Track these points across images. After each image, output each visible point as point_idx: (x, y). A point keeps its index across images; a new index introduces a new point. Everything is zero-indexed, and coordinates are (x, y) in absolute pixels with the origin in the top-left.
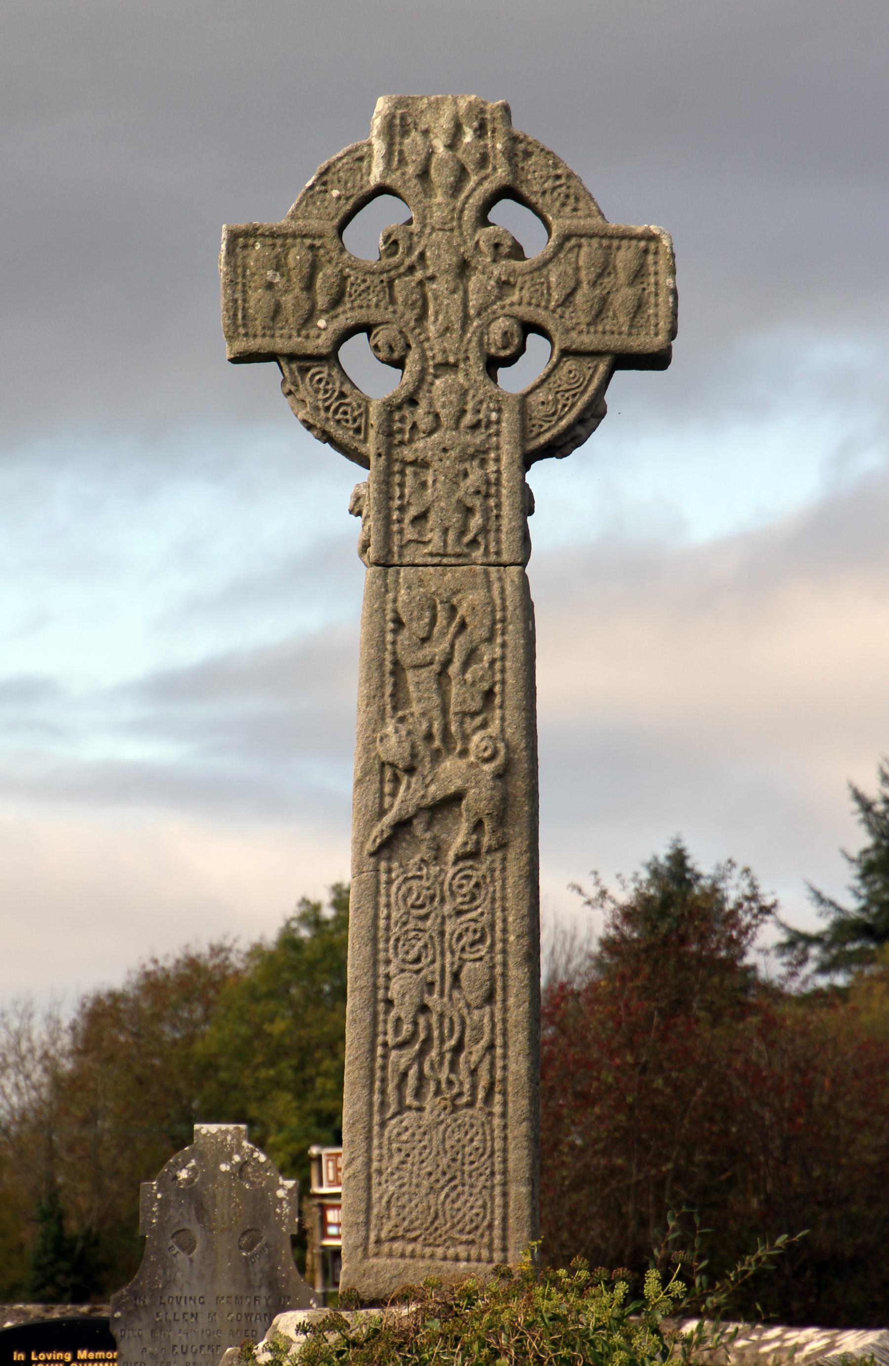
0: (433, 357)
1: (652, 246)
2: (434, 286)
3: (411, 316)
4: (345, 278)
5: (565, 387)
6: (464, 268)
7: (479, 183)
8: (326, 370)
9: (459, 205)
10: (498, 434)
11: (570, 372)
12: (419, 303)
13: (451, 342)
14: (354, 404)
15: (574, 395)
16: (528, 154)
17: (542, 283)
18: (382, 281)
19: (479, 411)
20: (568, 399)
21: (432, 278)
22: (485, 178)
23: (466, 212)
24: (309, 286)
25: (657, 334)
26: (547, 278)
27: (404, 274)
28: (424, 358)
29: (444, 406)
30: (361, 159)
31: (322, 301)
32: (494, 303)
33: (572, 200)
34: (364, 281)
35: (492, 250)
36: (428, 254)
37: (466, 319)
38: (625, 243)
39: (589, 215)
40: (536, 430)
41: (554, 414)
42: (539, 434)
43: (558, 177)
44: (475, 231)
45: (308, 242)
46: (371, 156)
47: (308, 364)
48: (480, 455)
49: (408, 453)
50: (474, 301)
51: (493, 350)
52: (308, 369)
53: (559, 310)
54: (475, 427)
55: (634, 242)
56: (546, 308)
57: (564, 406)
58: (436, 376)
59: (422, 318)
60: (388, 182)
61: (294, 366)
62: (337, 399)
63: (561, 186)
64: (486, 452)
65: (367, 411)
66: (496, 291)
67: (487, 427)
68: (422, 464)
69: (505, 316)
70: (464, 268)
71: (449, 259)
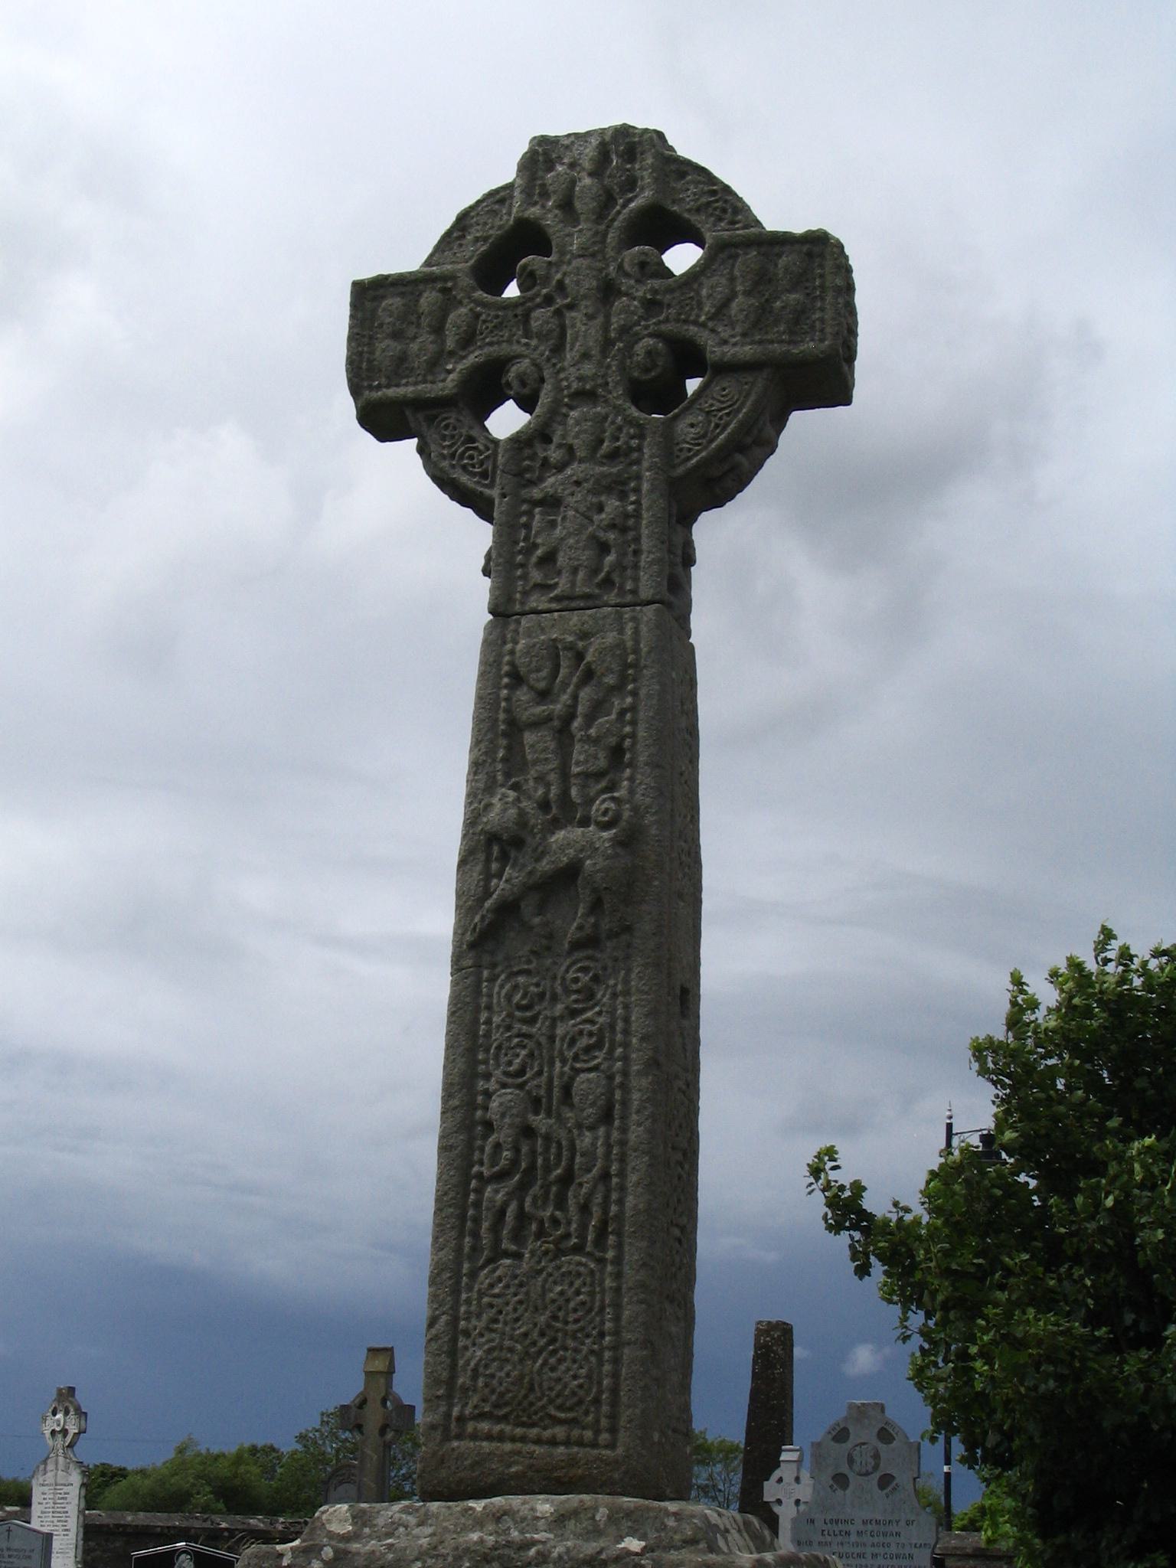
0: (568, 387)
1: (816, 250)
2: (574, 314)
3: (545, 349)
4: (477, 316)
5: (718, 405)
6: (608, 291)
7: (624, 206)
8: (454, 415)
9: (603, 227)
10: (638, 462)
11: (724, 389)
12: (555, 334)
13: (588, 369)
14: (481, 447)
15: (728, 414)
16: (682, 175)
17: (692, 298)
18: (516, 316)
19: (617, 439)
20: (721, 418)
21: (571, 307)
22: (631, 200)
23: (610, 235)
24: (438, 329)
25: (822, 340)
26: (698, 293)
27: (539, 306)
28: (559, 389)
29: (576, 437)
30: (502, 201)
31: (450, 344)
32: (638, 323)
33: (728, 216)
34: (497, 317)
35: (636, 268)
36: (567, 281)
37: (607, 344)
38: (787, 248)
39: (746, 227)
40: (684, 455)
41: (704, 436)
42: (689, 459)
43: (714, 193)
44: (619, 252)
45: (439, 285)
46: (512, 197)
47: (434, 412)
48: (618, 487)
49: (536, 493)
50: (616, 322)
51: (636, 374)
52: (436, 417)
53: (710, 324)
54: (613, 456)
55: (797, 247)
56: (695, 323)
57: (717, 426)
58: (571, 408)
59: (558, 349)
60: (526, 214)
61: (420, 416)
62: (463, 444)
63: (717, 201)
64: (624, 483)
65: (495, 454)
66: (641, 311)
67: (626, 455)
68: (552, 503)
69: (650, 335)
70: (608, 291)
71: (590, 283)
